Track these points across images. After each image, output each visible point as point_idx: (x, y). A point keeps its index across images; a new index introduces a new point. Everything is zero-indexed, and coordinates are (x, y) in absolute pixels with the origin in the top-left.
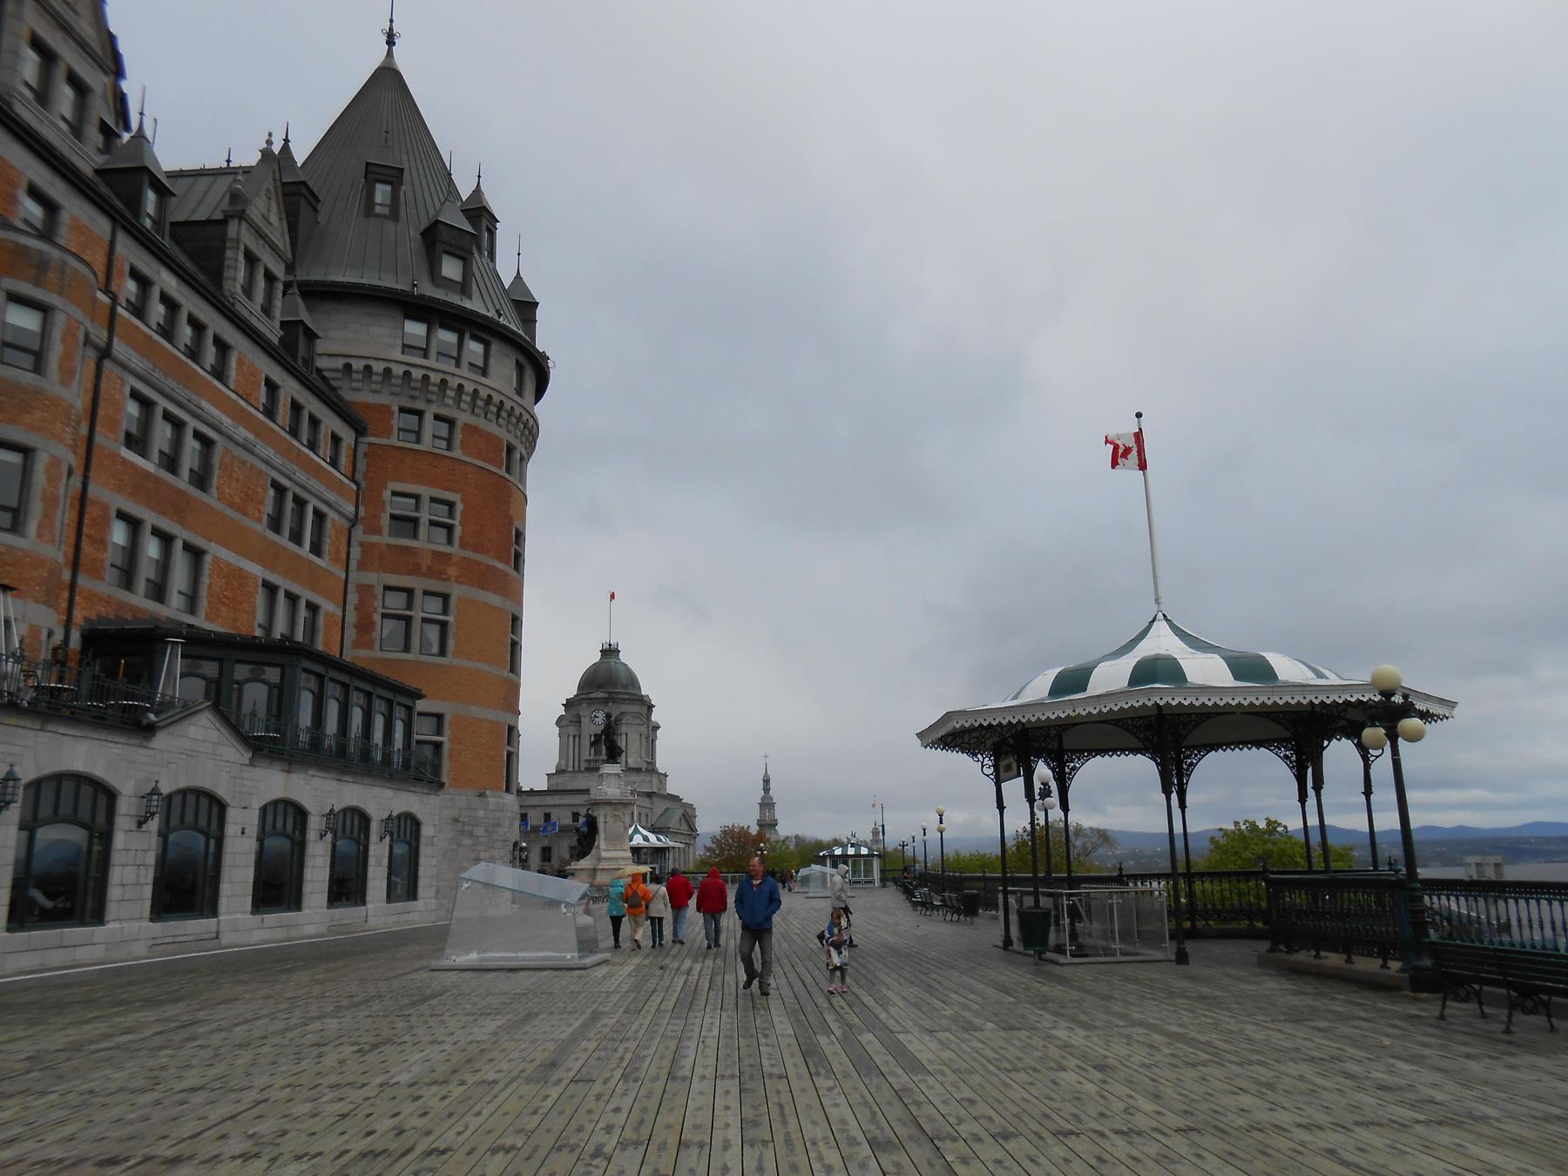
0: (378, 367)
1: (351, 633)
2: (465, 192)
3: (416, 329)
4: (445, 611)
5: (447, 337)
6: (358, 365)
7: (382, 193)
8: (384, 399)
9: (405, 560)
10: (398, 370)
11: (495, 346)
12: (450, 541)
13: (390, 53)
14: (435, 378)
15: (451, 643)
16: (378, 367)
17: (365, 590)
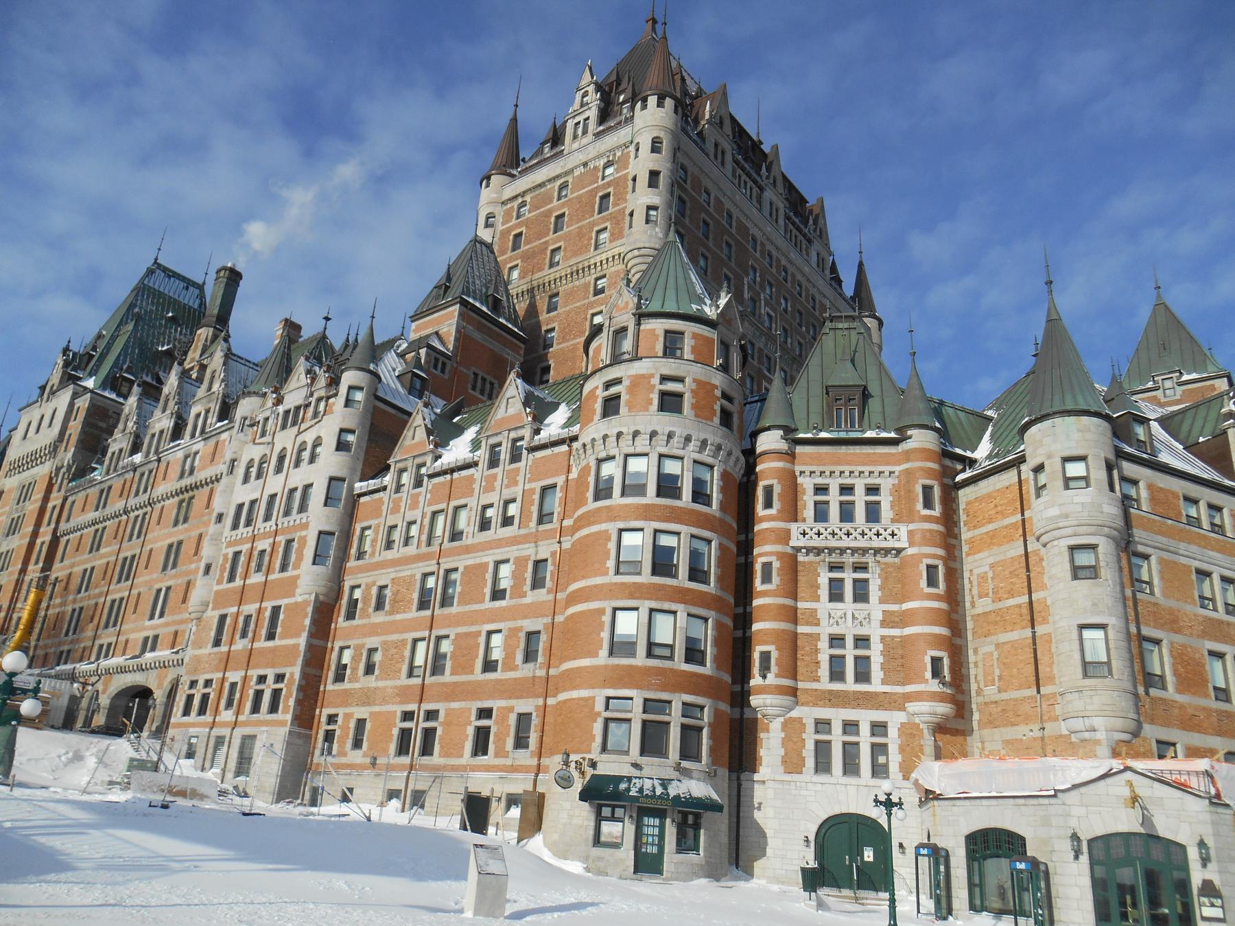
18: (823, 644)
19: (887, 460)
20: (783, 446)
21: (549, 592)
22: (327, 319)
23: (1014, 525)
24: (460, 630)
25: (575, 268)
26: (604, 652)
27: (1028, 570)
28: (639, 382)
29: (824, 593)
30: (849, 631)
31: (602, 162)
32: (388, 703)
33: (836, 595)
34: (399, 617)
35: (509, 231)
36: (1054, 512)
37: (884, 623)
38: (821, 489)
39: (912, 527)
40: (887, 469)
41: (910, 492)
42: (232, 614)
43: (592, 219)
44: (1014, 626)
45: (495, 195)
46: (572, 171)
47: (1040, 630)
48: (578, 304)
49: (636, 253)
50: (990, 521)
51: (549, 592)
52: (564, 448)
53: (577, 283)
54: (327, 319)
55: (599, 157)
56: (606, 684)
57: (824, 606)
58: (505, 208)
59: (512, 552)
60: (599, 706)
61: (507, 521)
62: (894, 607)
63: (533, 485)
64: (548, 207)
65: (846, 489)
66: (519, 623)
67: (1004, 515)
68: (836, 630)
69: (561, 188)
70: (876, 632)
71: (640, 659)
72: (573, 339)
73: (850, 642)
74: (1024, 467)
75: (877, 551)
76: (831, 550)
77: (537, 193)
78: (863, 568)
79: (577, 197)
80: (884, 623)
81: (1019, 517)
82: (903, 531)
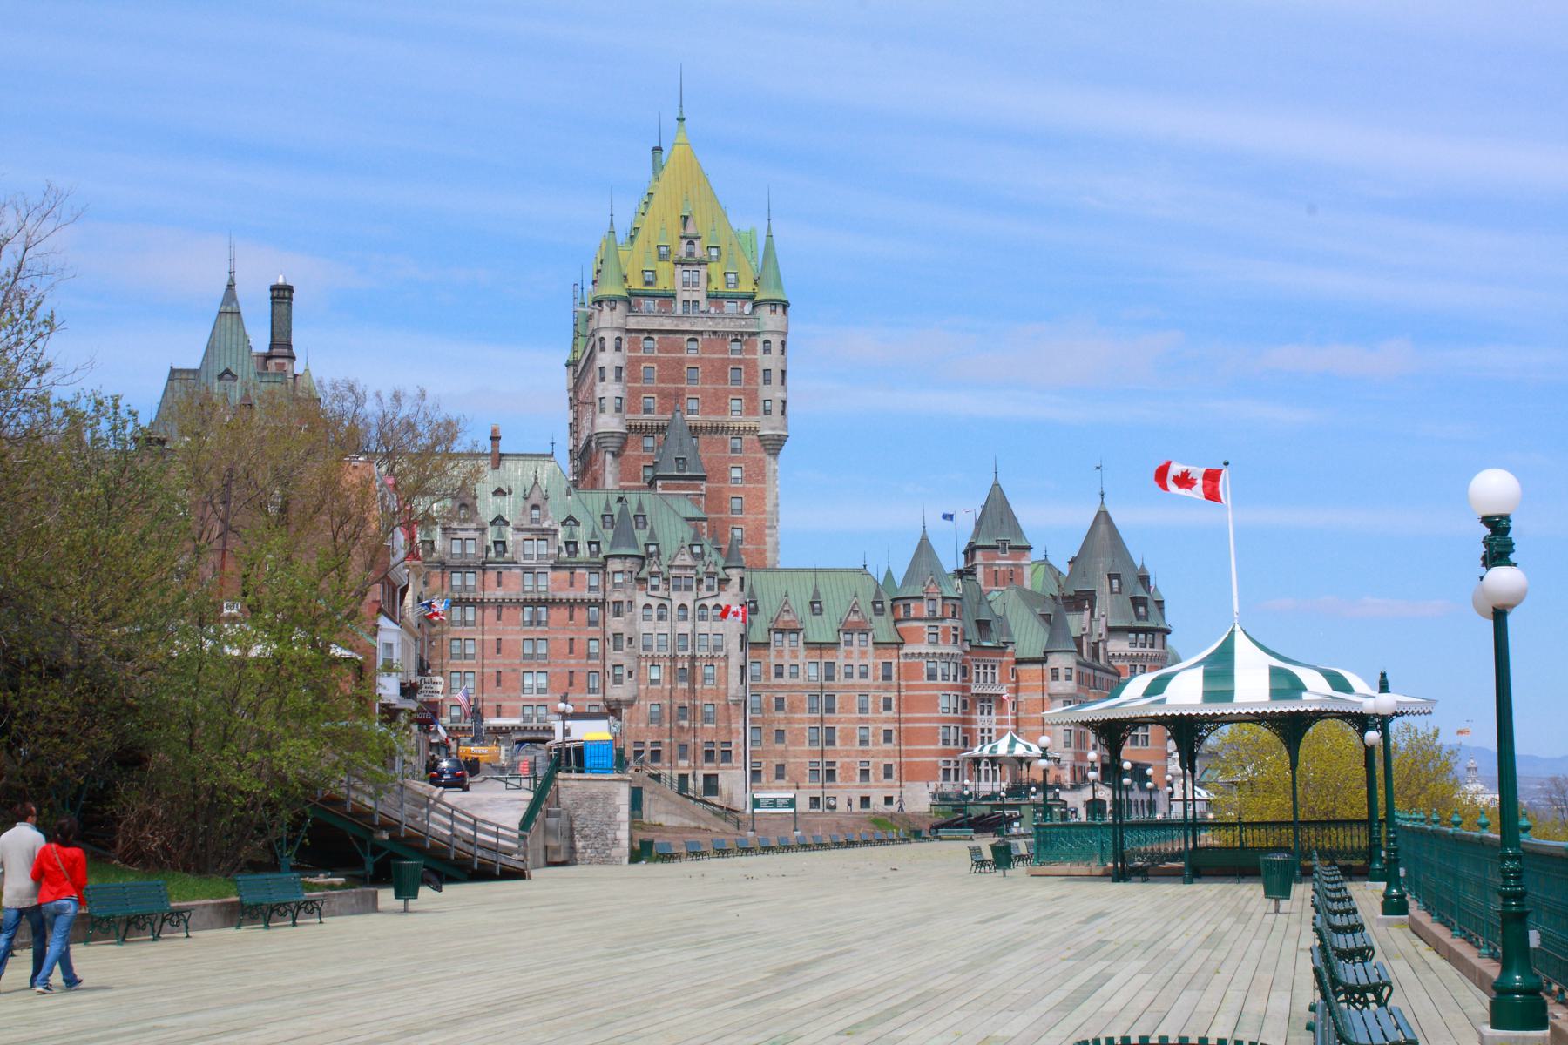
0: (1123, 654)
3: (1132, 636)
5: (1142, 636)
11: (1157, 635)
13: (1102, 502)
16: (1123, 654)
18: (979, 732)
20: (968, 649)
23: (1038, 686)
25: (715, 425)
26: (940, 744)
28: (946, 630)
30: (986, 726)
33: (982, 713)
34: (796, 716)
35: (639, 360)
36: (1061, 688)
37: (997, 724)
41: (1007, 670)
44: (1034, 724)
45: (621, 321)
46: (701, 333)
50: (1027, 681)
56: (942, 756)
60: (941, 764)
61: (864, 675)
68: (983, 727)
69: (689, 340)
70: (994, 727)
71: (952, 746)
72: (718, 483)
73: (986, 731)
76: (983, 695)
78: (990, 701)
79: (709, 359)
80: (997, 724)
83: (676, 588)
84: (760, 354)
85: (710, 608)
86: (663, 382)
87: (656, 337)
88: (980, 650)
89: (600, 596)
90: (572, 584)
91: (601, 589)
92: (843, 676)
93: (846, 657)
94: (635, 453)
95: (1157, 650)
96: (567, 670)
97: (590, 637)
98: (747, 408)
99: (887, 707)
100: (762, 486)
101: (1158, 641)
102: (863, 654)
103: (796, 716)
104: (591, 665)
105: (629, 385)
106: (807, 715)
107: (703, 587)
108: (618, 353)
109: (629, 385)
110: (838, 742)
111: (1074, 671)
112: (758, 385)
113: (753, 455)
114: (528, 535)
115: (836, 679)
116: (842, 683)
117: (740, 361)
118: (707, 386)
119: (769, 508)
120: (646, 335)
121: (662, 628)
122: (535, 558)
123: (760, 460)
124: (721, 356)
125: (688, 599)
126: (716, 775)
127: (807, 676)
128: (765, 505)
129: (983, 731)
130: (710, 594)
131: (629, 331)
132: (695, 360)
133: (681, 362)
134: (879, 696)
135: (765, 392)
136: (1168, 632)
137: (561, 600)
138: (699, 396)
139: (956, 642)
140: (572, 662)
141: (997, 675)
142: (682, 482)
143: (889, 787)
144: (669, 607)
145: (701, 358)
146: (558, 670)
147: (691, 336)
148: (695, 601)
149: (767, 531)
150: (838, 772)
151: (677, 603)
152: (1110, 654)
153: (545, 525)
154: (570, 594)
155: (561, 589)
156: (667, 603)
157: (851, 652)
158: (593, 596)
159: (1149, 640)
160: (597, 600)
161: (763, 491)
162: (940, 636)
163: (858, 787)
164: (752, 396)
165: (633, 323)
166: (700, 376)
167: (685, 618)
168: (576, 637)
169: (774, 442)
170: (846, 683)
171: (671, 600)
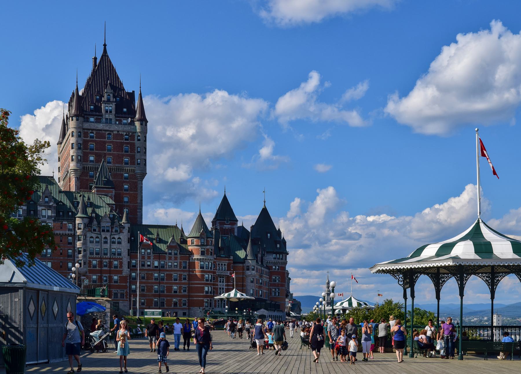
0: (271, 261)
1: (269, 294)
2: (277, 229)
3: (274, 255)
4: (279, 290)
5: (278, 255)
6: (269, 261)
7: (269, 235)
8: (271, 265)
9: (274, 285)
10: (273, 262)
11: (283, 255)
12: (279, 282)
14: (277, 262)
15: (280, 294)
16: (271, 261)
17: (271, 289)
18: (219, 289)
19: (226, 260)
20: (215, 257)
21: (187, 281)
22: (53, 172)
24: (167, 285)
27: (243, 280)
28: (208, 250)
29: (219, 281)
30: (222, 287)
31: (125, 134)
32: (150, 297)
34: (149, 281)
35: (88, 141)
36: (250, 273)
37: (225, 286)
38: (219, 264)
39: (230, 272)
40: (227, 262)
42: (98, 276)
43: (122, 153)
46: (113, 131)
47: (244, 288)
48: (119, 180)
49: (142, 174)
51: (187, 281)
52: (188, 255)
53: (118, 172)
54: (53, 172)
55: (124, 132)
57: (219, 283)
58: (84, 131)
59: (179, 273)
62: (226, 284)
63: (181, 261)
64: (104, 140)
65: (222, 265)
66: (182, 285)
67: (240, 270)
69: (108, 134)
71: (209, 294)
73: (222, 289)
74: (244, 264)
75: (226, 275)
76: (220, 275)
77: (98, 132)
78: (223, 278)
79: (116, 142)
80: (225, 286)
81: (242, 271)
82: (229, 272)
83: (103, 231)
84: (136, 141)
85: (116, 239)
86: (97, 150)
87: (95, 132)
88: (220, 258)
89: (73, 232)
90: (61, 228)
91: (73, 230)
92: (167, 267)
93: (169, 259)
94: (87, 178)
95: (283, 261)
96: (59, 261)
97: (68, 249)
98: (130, 162)
99: (185, 279)
100: (136, 193)
101: (284, 258)
102: (176, 258)
103: (149, 281)
104: (69, 259)
105: (84, 151)
106: (154, 281)
107: (114, 230)
108: (80, 139)
109: (84, 151)
110: (165, 292)
111: (255, 267)
112: (135, 153)
113: (133, 181)
114: (44, 208)
115: (165, 267)
116: (167, 269)
117: (128, 143)
118: (115, 153)
119: (139, 201)
120: (91, 131)
121: (98, 246)
122: (47, 217)
123: (136, 182)
124: (120, 141)
125: (108, 235)
126: (118, 303)
127: (154, 266)
128: (137, 200)
129: (220, 288)
130: (116, 233)
131: (84, 129)
132: (111, 142)
133: (105, 143)
134: (182, 274)
135: (137, 156)
136: (288, 254)
137: (57, 234)
138: (112, 157)
139: (211, 255)
140: (62, 258)
141: (226, 268)
142: (105, 189)
143: (185, 309)
144: (100, 238)
145: (113, 141)
146: (56, 261)
147: (109, 132)
148: (110, 236)
149: (138, 210)
150: (165, 302)
151: (103, 236)
152: (267, 261)
153: (51, 204)
154: (61, 232)
155: (57, 230)
156: (99, 236)
157: (171, 257)
158: (70, 232)
159: (281, 257)
160: (71, 234)
161: (137, 194)
162: (205, 252)
163: (173, 309)
164: (132, 158)
165: (86, 125)
166: (112, 148)
167: (106, 242)
168: (63, 248)
169: (141, 176)
170: (169, 269)
171: (101, 235)
